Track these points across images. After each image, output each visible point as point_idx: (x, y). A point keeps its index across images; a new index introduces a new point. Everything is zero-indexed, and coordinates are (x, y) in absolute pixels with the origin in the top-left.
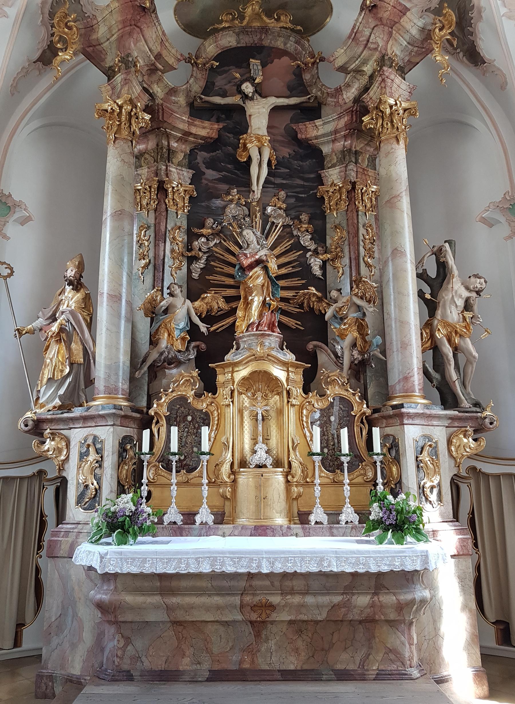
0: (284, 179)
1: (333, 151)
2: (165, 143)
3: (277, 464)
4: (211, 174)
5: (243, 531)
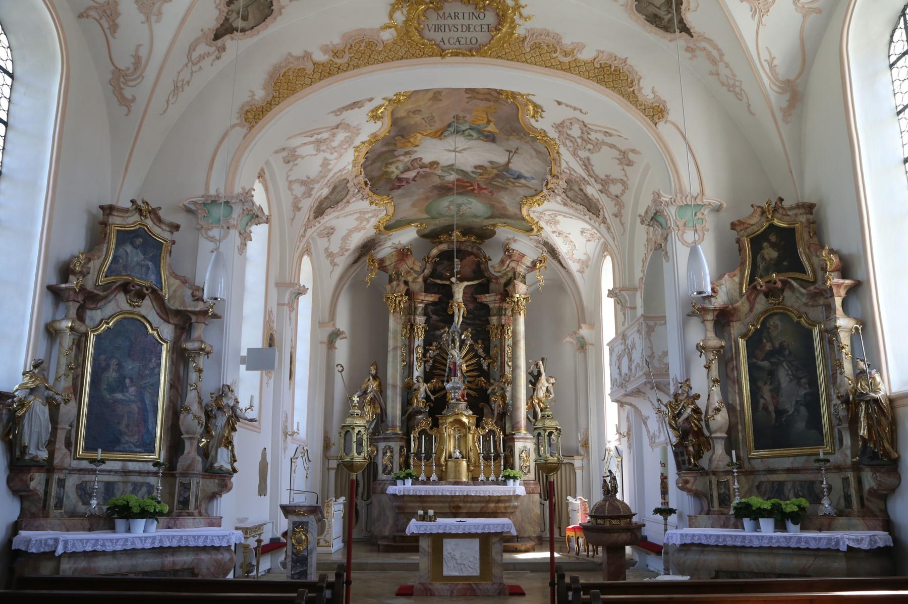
0: (470, 320)
2: (413, 305)
3: (463, 458)
4: (434, 317)
5: (450, 483)
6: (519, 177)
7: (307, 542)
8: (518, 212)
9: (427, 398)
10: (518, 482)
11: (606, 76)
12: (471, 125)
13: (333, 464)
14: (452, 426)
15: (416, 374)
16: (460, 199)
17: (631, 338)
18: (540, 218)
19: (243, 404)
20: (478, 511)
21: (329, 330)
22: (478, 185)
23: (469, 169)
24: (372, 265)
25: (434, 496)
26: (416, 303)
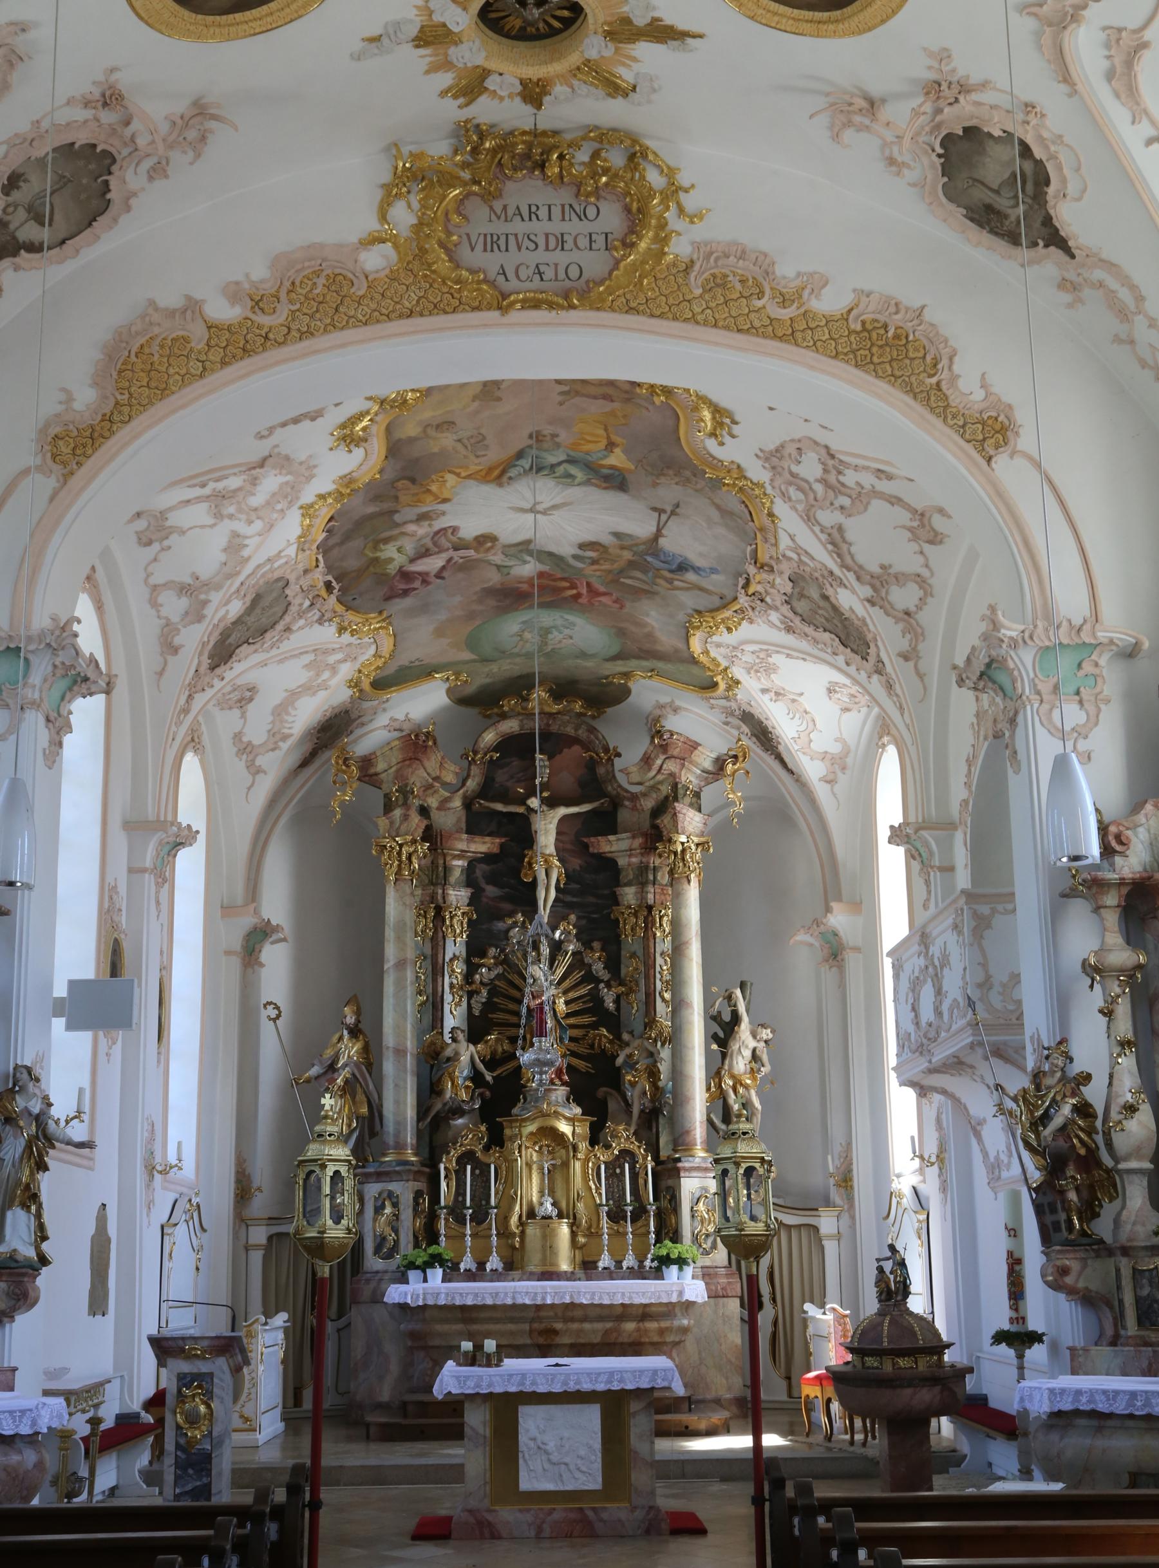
0: (574, 896)
1: (629, 865)
2: (441, 862)
3: (560, 1216)
4: (491, 890)
5: (531, 1277)
6: (683, 567)
7: (211, 1421)
8: (681, 645)
9: (476, 1078)
10: (689, 1271)
11: (874, 350)
12: (572, 453)
13: (259, 1235)
14: (535, 1143)
15: (450, 1022)
16: (547, 618)
17: (939, 942)
18: (732, 659)
19: (61, 1109)
20: (595, 1341)
21: (247, 922)
22: (589, 585)
23: (566, 550)
24: (344, 772)
25: (494, 1307)
26: (448, 858)
